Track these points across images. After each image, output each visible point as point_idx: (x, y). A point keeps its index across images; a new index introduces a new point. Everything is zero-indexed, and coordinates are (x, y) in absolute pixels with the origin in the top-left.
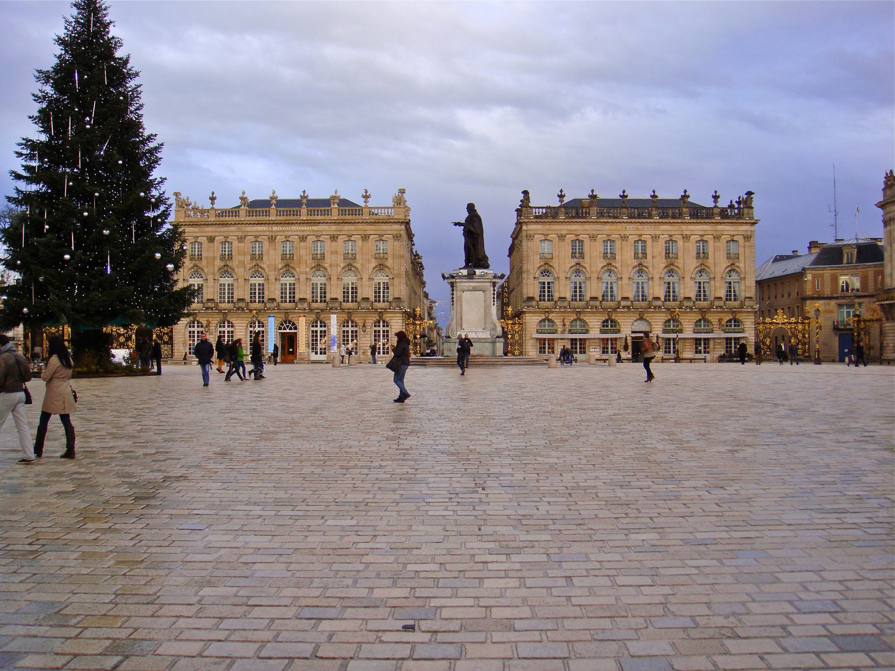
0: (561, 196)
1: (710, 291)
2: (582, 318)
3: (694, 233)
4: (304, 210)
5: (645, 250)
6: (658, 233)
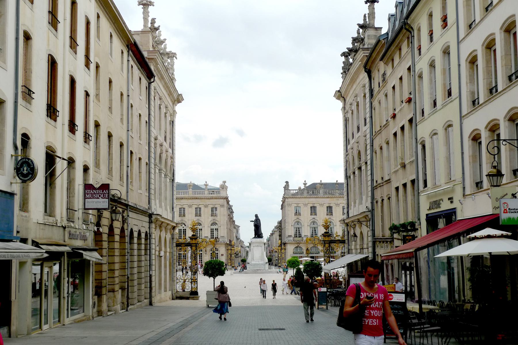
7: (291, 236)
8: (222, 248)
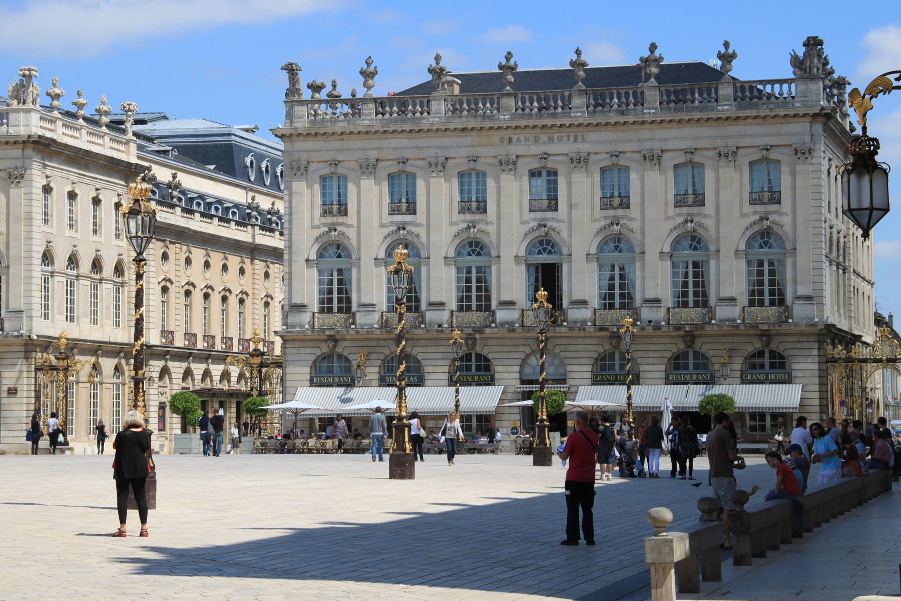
0: (368, 75)
3: (670, 145)
6: (584, 148)
7: (442, 304)
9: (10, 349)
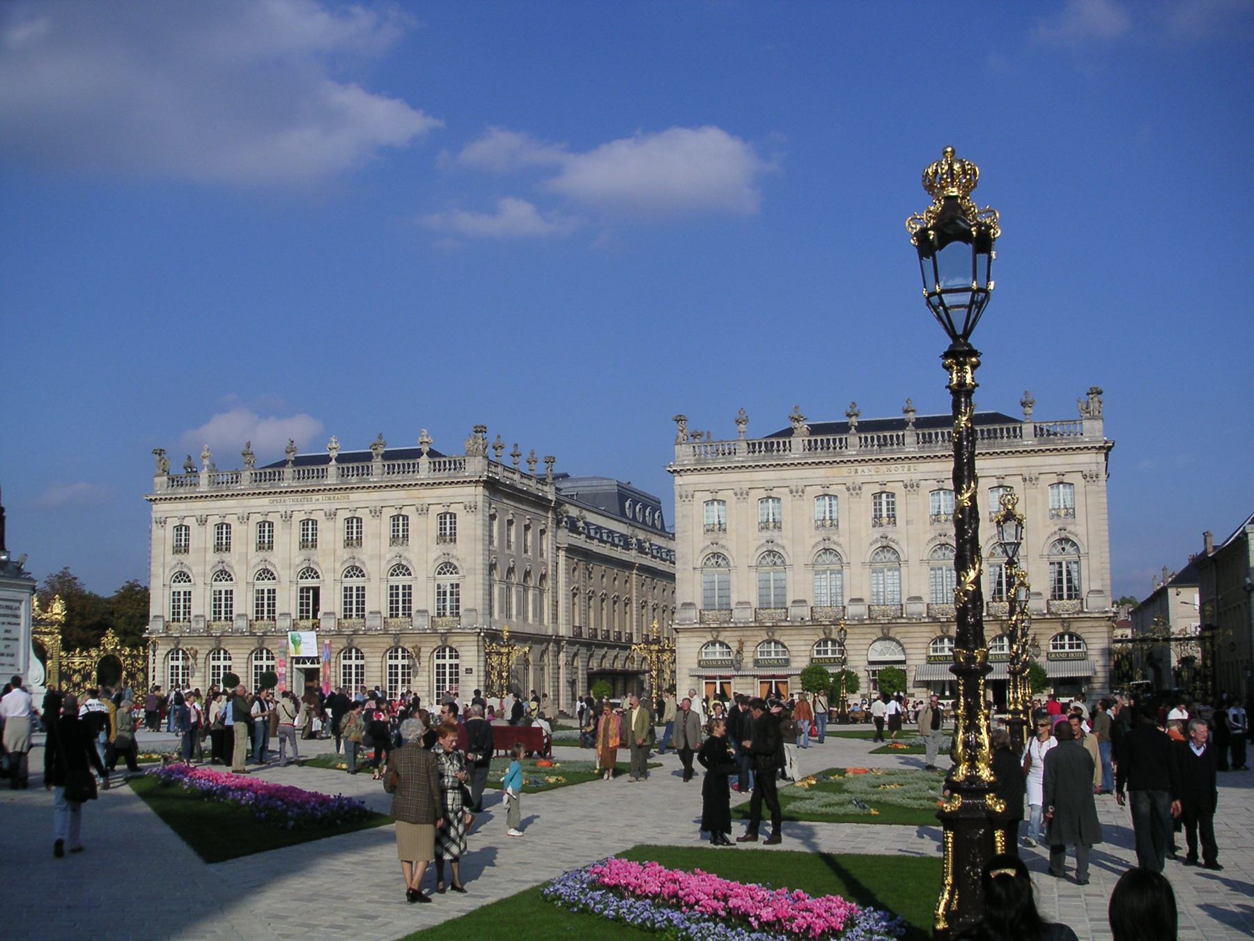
1: (1080, 580)
2: (777, 638)
4: (332, 468)
5: (893, 510)
6: (916, 477)
8: (467, 648)
9: (467, 638)
